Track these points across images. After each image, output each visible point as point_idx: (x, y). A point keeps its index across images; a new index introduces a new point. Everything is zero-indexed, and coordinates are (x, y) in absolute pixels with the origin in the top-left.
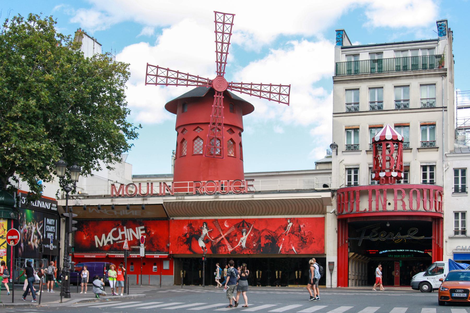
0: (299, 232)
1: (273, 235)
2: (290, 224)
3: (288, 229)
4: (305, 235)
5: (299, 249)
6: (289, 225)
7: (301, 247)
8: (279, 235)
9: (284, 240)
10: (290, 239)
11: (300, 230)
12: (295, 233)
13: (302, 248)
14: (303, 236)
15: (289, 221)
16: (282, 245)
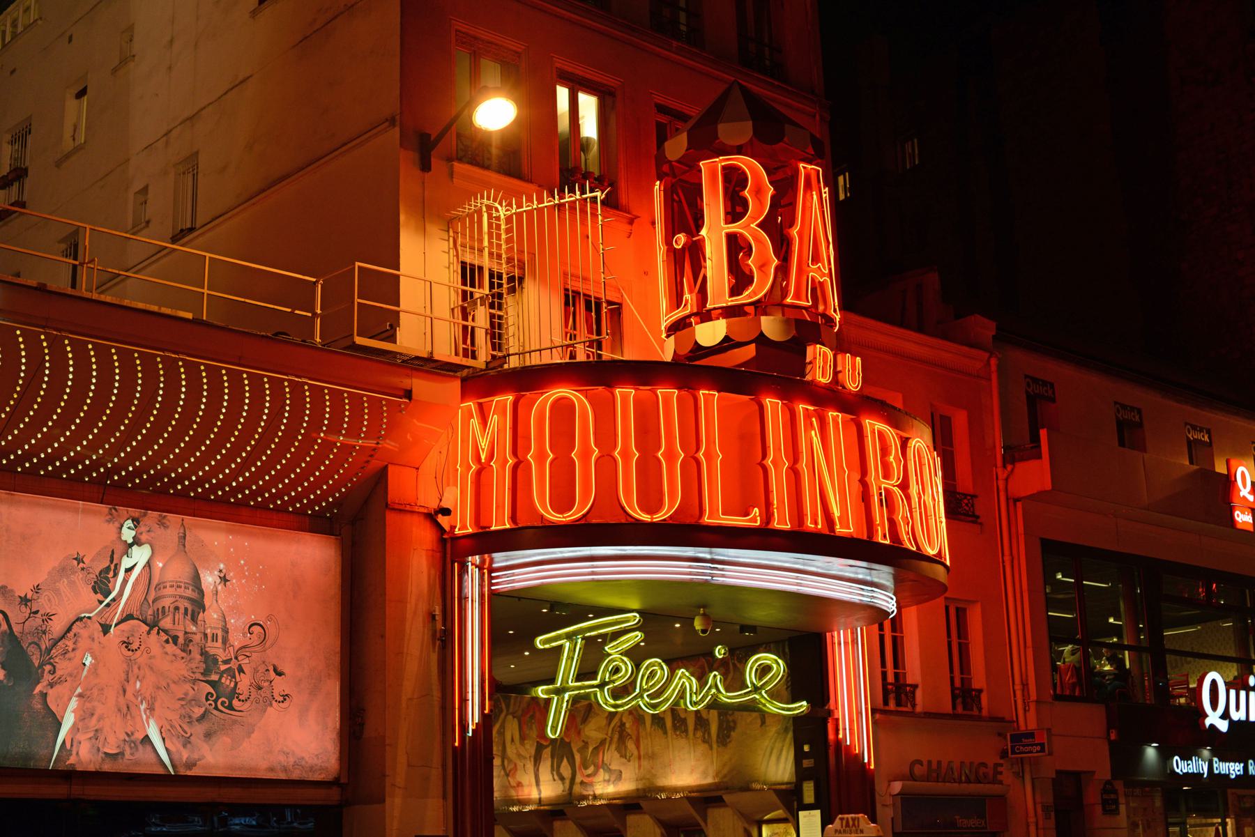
0: (194, 620)
1: (17, 615)
2: (135, 548)
3: (125, 589)
4: (225, 641)
5: (187, 742)
6: (126, 563)
7: (199, 729)
8: (57, 626)
9: (94, 668)
10: (129, 662)
11: (198, 605)
12: (166, 623)
13: (208, 735)
14: (215, 649)
15: (128, 535)
16: (74, 703)
